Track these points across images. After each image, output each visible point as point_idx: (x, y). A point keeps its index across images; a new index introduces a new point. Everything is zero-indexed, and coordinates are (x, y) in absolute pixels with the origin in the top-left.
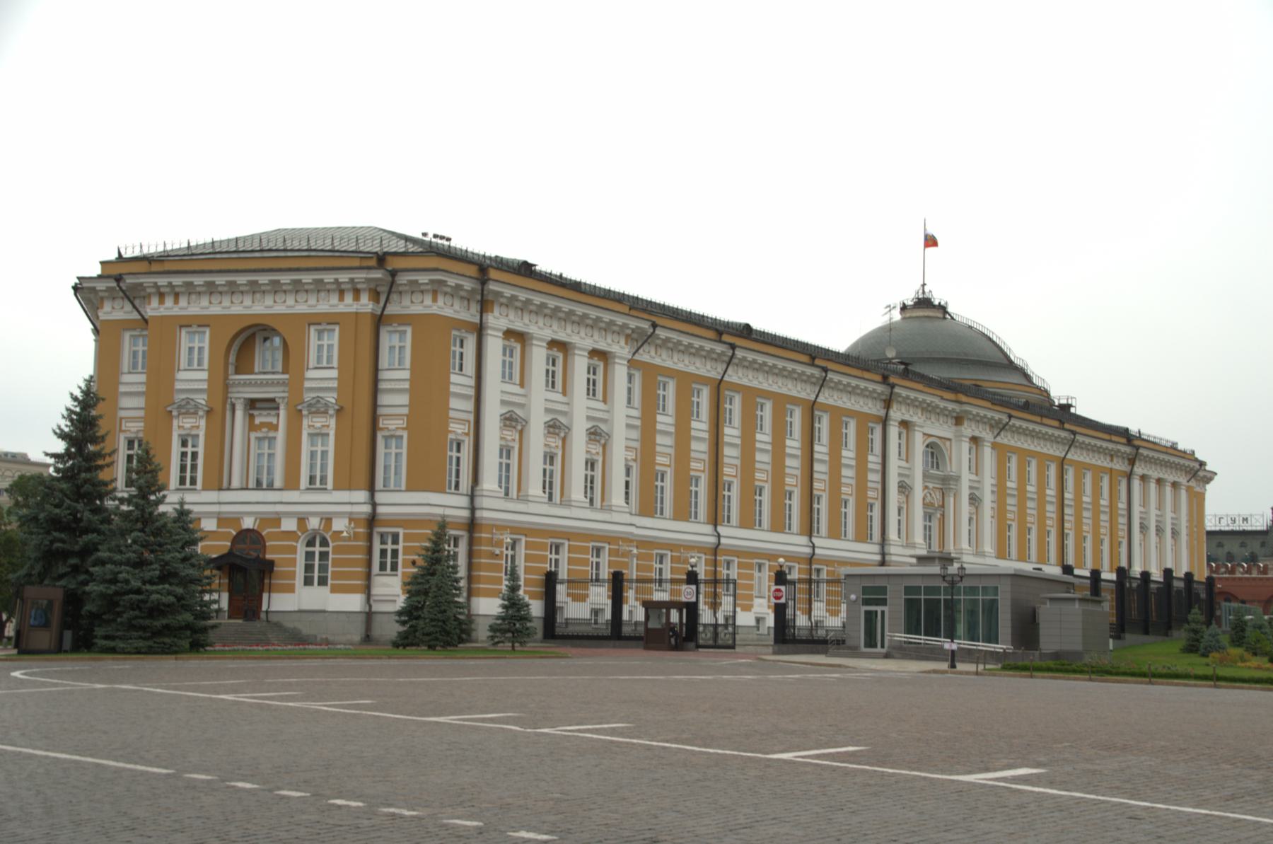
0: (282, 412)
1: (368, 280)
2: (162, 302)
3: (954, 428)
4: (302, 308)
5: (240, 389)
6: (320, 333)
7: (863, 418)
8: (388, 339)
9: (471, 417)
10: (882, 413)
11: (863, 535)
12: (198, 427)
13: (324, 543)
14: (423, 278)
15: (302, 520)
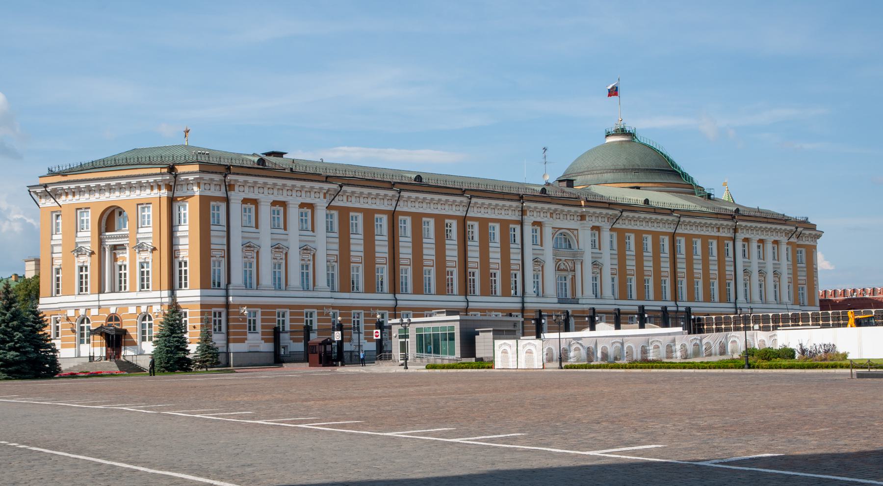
0: (128, 251)
3: (579, 222)
7: (505, 224)
9: (225, 247)
10: (519, 218)
11: (506, 293)
13: (150, 319)
14: (191, 178)
15: (138, 307)
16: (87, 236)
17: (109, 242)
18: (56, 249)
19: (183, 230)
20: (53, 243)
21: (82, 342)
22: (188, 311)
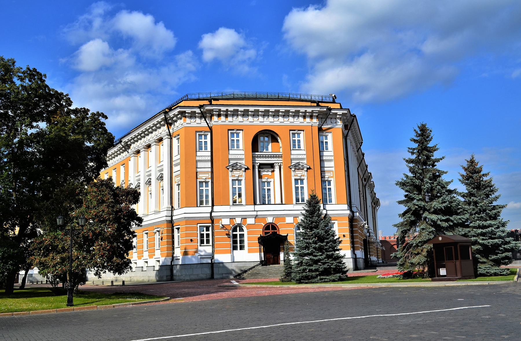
5: (259, 159)
6: (293, 134)
12: (241, 176)
16: (240, 152)
17: (259, 161)
18: (200, 165)
19: (328, 154)
20: (198, 158)
21: (235, 248)
22: (336, 222)
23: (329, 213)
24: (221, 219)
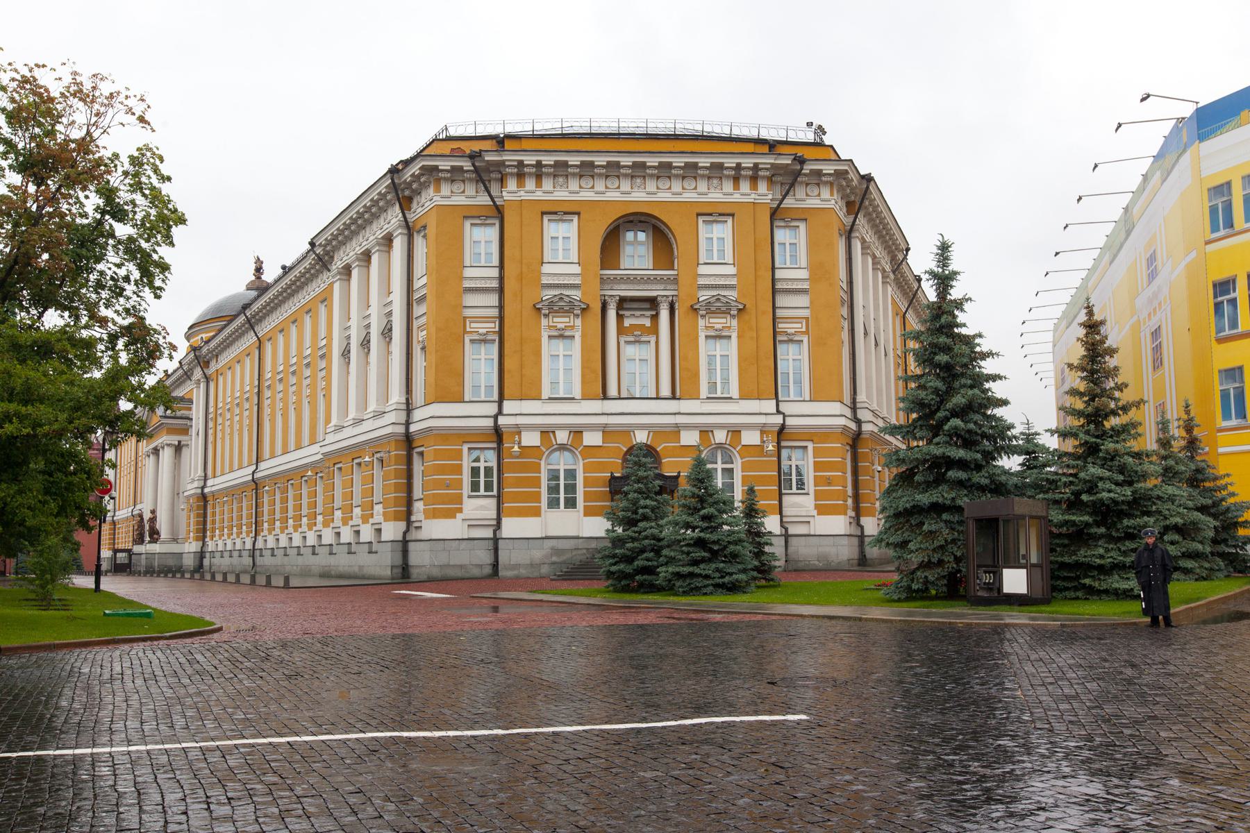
1: (772, 164)
2: (521, 184)
4: (690, 196)
8: (781, 235)
15: (705, 432)
23: (790, 421)
24: (519, 433)
